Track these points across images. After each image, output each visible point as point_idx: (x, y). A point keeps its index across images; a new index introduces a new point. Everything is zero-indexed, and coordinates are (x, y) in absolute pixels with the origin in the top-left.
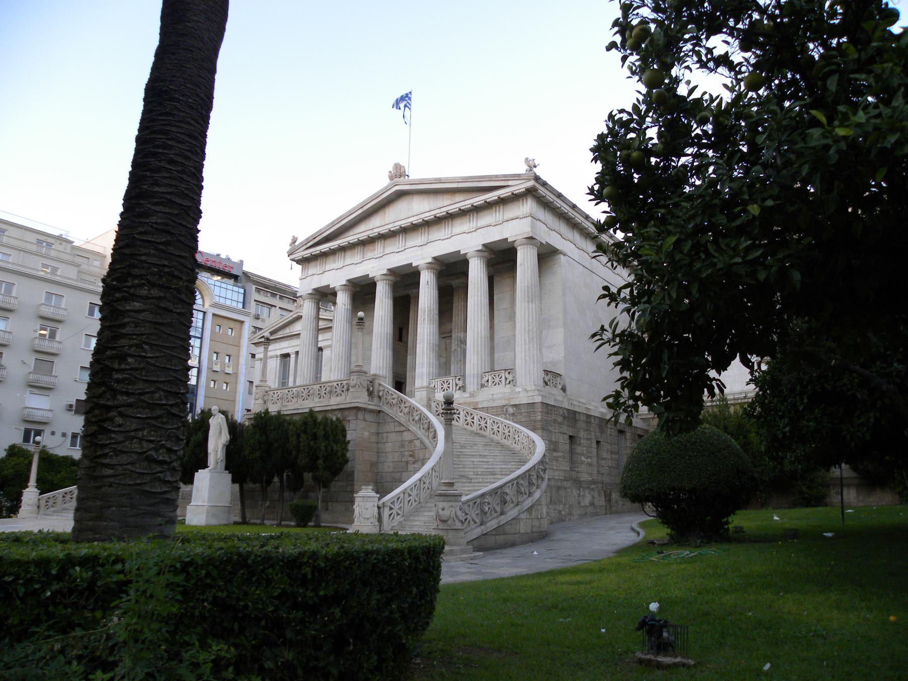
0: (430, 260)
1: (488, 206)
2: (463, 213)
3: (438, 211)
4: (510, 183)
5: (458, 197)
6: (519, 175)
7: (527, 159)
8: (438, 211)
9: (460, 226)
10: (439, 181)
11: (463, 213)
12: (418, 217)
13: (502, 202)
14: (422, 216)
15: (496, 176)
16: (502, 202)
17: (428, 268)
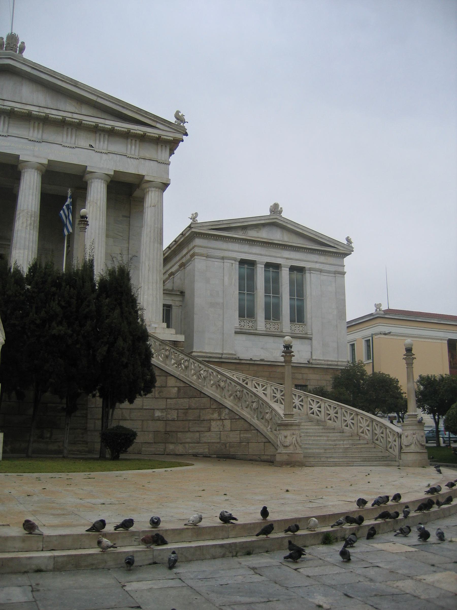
0: (46, 162)
1: (127, 136)
2: (95, 130)
3: (70, 115)
4: (158, 125)
5: (85, 110)
6: (170, 123)
7: (178, 112)
8: (70, 115)
9: (84, 140)
10: (75, 84)
11: (95, 130)
12: (41, 110)
13: (143, 139)
14: (48, 111)
15: (146, 112)
16: (143, 139)
17: (37, 169)
